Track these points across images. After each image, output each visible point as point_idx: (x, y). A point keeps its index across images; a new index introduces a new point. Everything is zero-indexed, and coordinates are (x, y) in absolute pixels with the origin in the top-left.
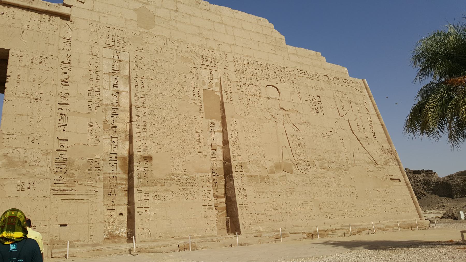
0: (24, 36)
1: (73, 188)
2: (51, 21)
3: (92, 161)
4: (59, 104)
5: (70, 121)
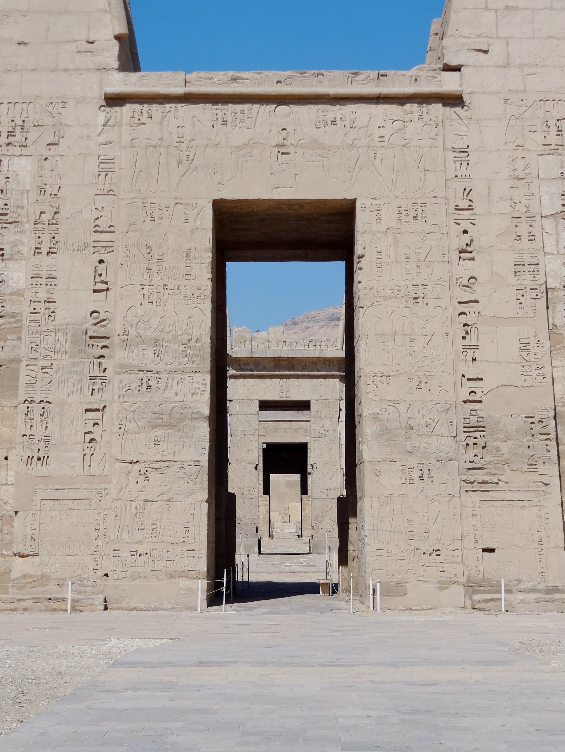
0: (378, 162)
1: (502, 478)
2: (425, 116)
3: (532, 420)
4: (459, 303)
5: (483, 337)
